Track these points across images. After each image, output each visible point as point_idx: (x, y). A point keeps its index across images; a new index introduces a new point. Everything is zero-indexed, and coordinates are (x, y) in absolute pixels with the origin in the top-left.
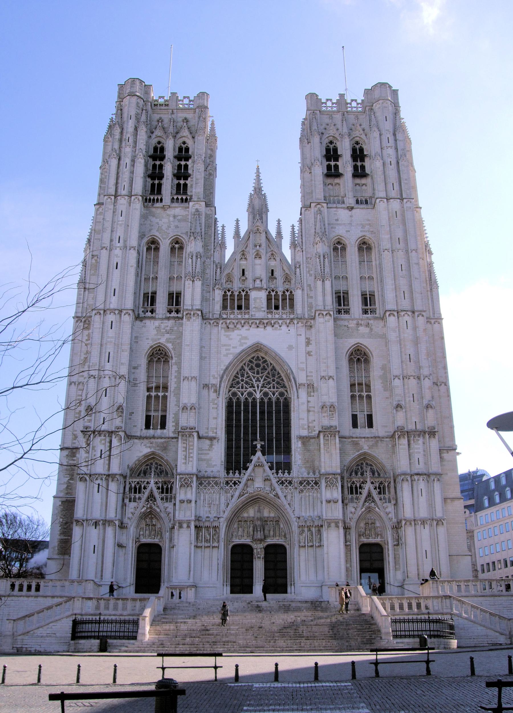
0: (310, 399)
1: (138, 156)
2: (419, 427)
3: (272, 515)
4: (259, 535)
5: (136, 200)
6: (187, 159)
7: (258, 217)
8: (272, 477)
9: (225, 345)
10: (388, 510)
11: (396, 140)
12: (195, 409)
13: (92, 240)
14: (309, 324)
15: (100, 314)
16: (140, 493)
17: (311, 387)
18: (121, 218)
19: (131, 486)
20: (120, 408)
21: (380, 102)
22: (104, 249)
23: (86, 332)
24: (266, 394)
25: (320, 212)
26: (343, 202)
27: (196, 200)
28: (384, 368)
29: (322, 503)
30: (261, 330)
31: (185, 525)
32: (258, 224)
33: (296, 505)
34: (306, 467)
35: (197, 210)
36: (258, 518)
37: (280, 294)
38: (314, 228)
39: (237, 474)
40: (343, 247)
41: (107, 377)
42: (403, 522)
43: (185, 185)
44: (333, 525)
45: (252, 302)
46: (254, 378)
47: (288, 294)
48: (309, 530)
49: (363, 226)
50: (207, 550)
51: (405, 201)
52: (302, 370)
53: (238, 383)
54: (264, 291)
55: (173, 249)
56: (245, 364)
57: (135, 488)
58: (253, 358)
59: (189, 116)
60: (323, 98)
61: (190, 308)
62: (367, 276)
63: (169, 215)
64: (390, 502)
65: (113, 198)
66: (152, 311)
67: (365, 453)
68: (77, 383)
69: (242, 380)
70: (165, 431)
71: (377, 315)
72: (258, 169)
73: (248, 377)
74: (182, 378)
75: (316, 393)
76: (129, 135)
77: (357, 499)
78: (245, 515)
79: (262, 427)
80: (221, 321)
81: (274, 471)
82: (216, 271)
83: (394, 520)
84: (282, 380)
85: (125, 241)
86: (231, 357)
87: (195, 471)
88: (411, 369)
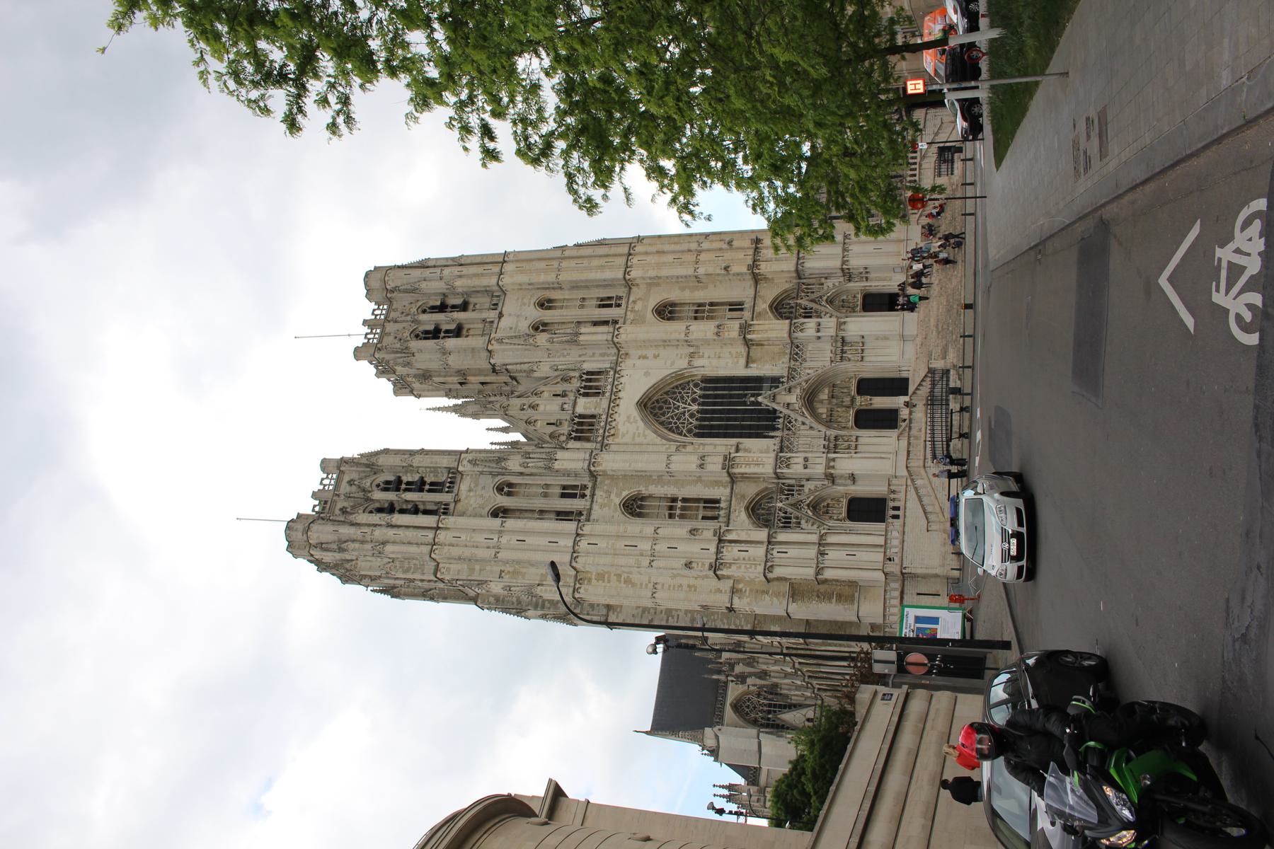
0: (706, 356)
1: (389, 521)
2: (751, 252)
3: (826, 391)
4: (847, 400)
5: (443, 521)
6: (399, 481)
7: (490, 406)
8: (786, 385)
9: (634, 438)
10: (831, 286)
11: (435, 266)
12: (704, 456)
13: (481, 579)
14: (623, 357)
15: (577, 557)
16: (790, 518)
17: (692, 355)
18: (463, 538)
19: (782, 527)
20: (693, 532)
21: (387, 278)
22: (498, 555)
23: (594, 581)
24: (694, 400)
25: (500, 341)
26: (492, 322)
27: (456, 463)
28: (683, 289)
29: (819, 338)
30: (621, 402)
31: (832, 464)
32: (498, 406)
33: (819, 364)
34: (779, 360)
35: (469, 461)
36: (829, 404)
37: (584, 383)
38: (517, 347)
39: (781, 420)
40: (542, 326)
41: (654, 547)
42: (844, 267)
43: (432, 484)
44: (842, 327)
45: (588, 412)
46: (673, 411)
47: (585, 377)
48: (845, 353)
49: (524, 304)
50: (859, 446)
51: (506, 259)
52: (673, 363)
53: (678, 428)
54: (578, 400)
55: (509, 494)
56: (657, 421)
57: (785, 523)
58: (651, 413)
59: (346, 478)
60: (360, 341)
61: (587, 462)
62: (579, 303)
63: (467, 497)
64: (823, 284)
65: (435, 547)
66: (580, 514)
67: (771, 307)
68: (654, 590)
69: (675, 423)
70: (723, 498)
71: (624, 295)
72: (430, 409)
73: (673, 418)
74: (668, 470)
75: (701, 351)
76: (359, 532)
77: (816, 312)
78: (824, 416)
79: (730, 404)
80: (606, 441)
81: (780, 385)
82: (542, 448)
83: (842, 279)
84: (680, 385)
85: (492, 531)
86: (648, 432)
87: (773, 455)
88: (692, 258)
